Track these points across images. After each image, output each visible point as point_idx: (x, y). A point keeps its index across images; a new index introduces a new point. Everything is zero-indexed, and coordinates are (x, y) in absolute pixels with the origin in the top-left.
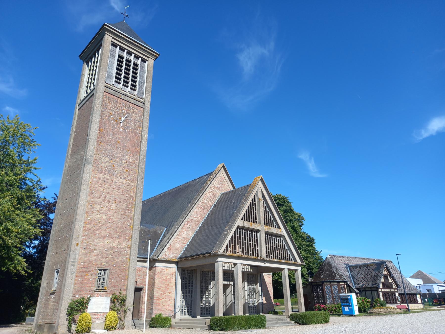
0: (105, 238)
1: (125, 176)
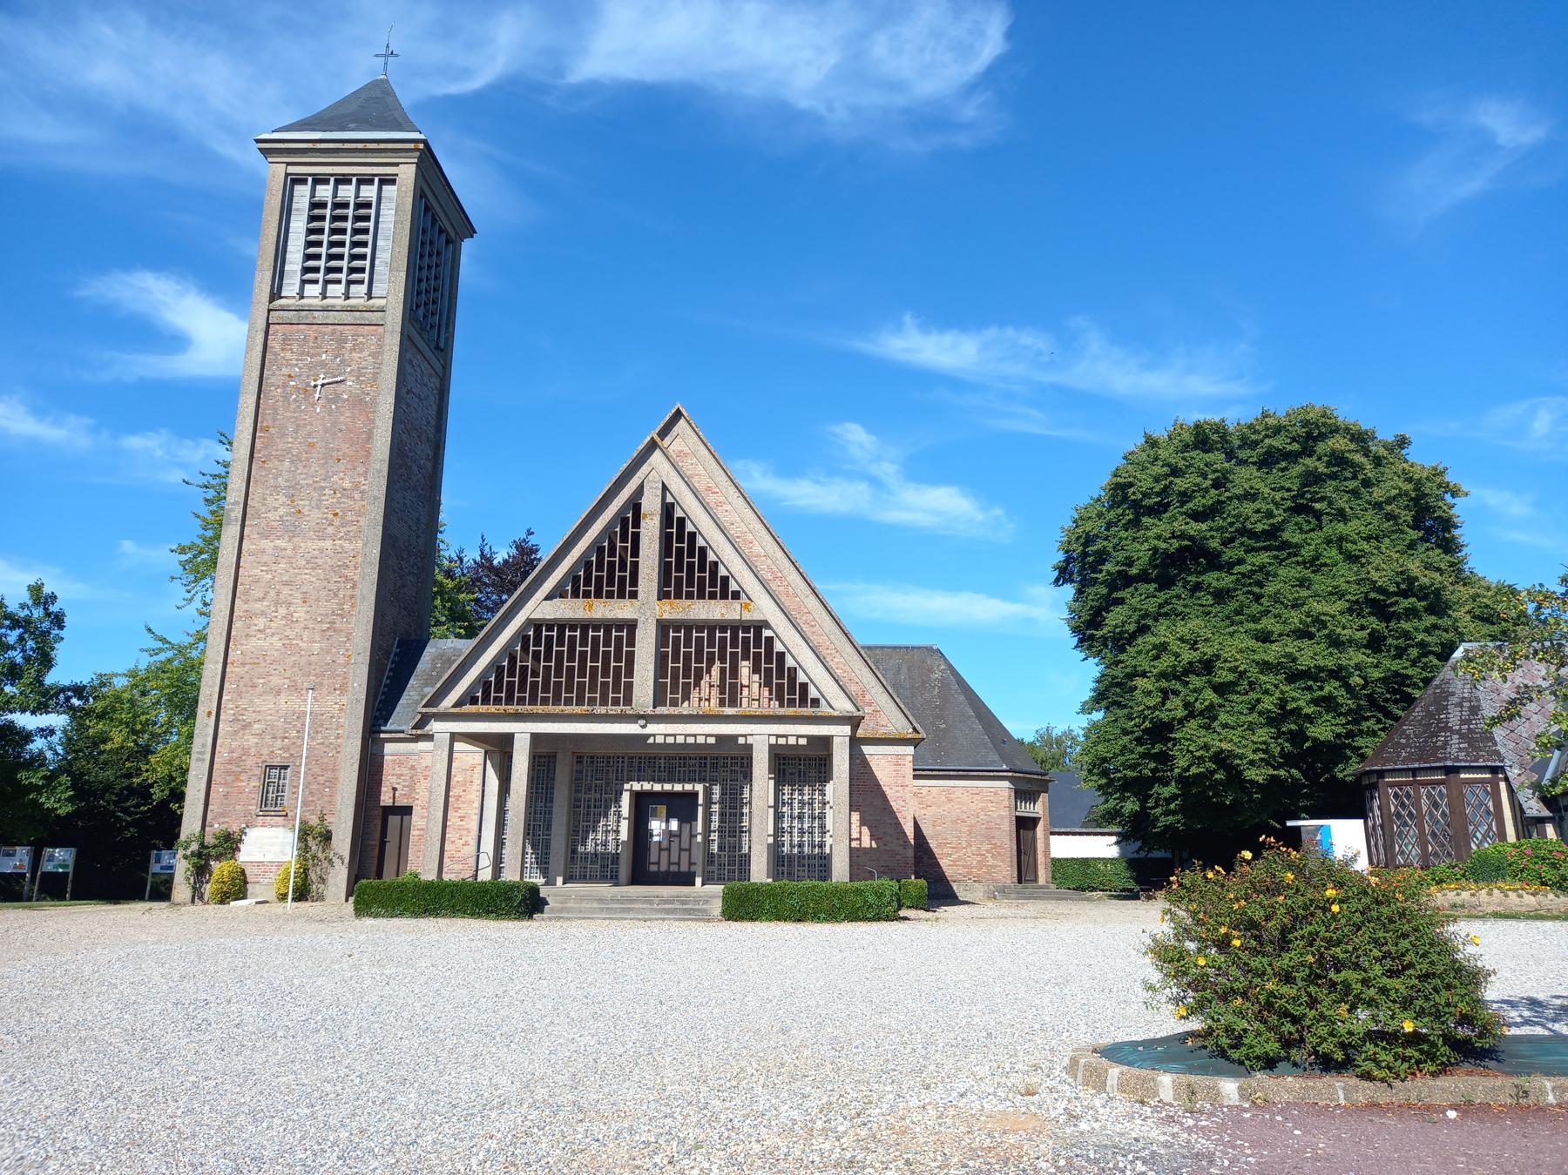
0: (278, 693)
1: (330, 530)
